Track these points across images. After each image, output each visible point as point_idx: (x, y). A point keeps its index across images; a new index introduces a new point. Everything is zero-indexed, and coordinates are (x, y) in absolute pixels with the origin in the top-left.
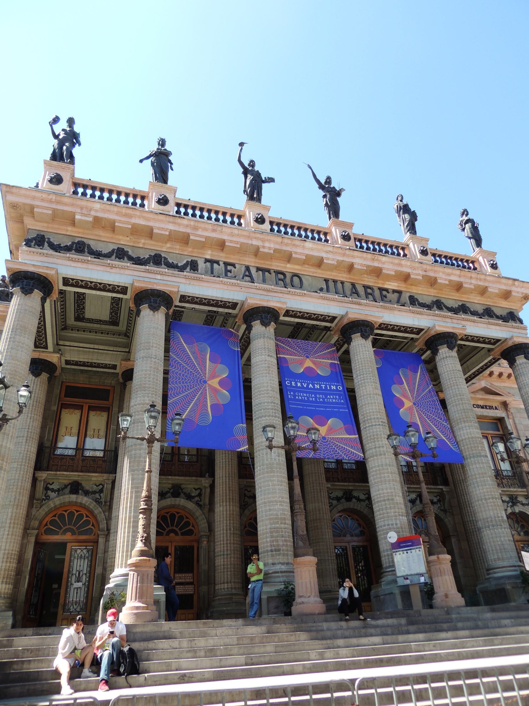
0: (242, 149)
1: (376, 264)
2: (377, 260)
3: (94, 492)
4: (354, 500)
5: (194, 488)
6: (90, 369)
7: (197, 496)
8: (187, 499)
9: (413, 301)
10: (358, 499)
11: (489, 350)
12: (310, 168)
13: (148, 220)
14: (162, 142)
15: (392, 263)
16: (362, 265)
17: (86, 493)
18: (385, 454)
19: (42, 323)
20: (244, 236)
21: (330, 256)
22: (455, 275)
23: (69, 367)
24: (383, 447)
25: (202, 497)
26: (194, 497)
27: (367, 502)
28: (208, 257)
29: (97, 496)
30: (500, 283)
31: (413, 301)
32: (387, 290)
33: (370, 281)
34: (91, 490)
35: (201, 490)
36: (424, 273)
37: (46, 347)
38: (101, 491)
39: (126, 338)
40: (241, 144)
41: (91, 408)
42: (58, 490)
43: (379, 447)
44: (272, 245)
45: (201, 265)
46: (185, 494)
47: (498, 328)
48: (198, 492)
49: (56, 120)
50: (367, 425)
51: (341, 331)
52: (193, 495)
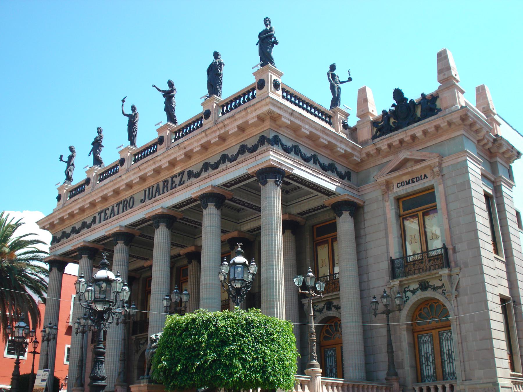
0: (123, 106)
1: (158, 165)
2: (156, 161)
9: (191, 175)
12: (154, 86)
13: (71, 208)
14: (99, 131)
15: (164, 157)
16: (151, 171)
20: (99, 192)
21: (135, 176)
22: (203, 137)
28: (99, 210)
30: (236, 120)
31: (191, 175)
32: (175, 176)
33: (165, 175)
36: (184, 151)
40: (123, 101)
44: (111, 189)
45: (98, 217)
47: (244, 164)
49: (61, 157)
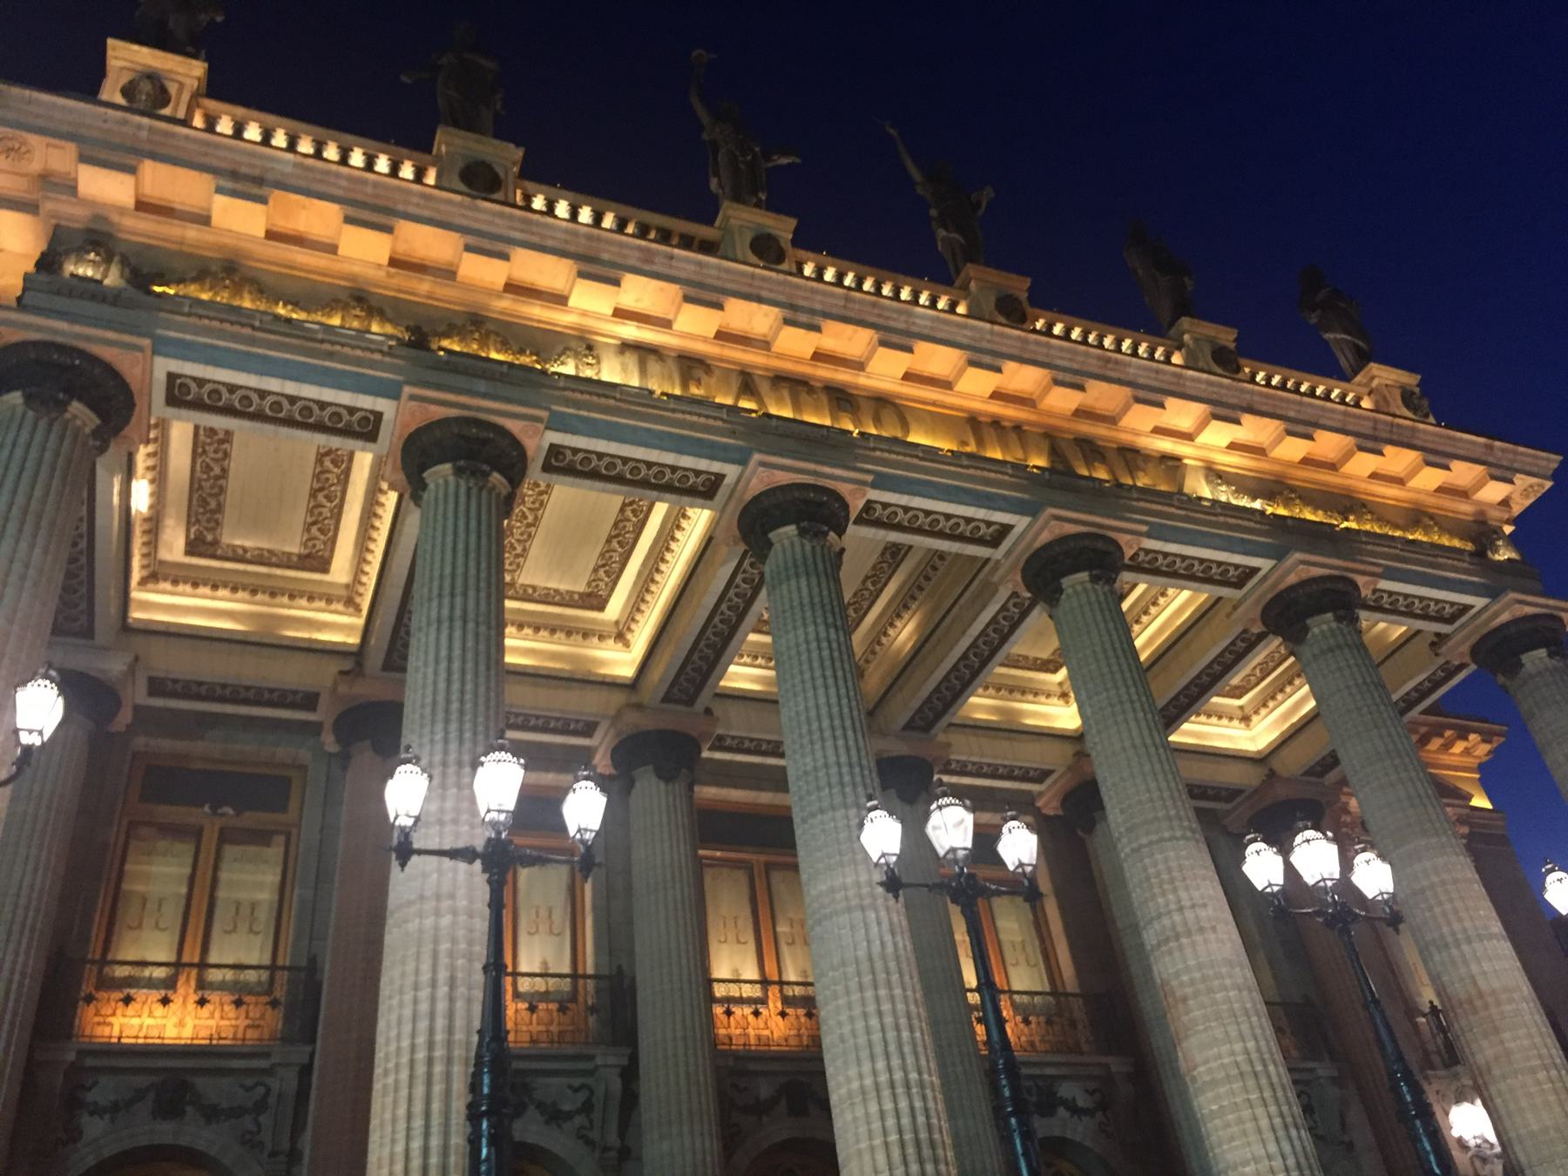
3: (237, 1112)
4: (1062, 1111)
5: (570, 1087)
6: (229, 709)
7: (578, 1112)
8: (547, 1123)
10: (1075, 1110)
11: (1441, 638)
17: (212, 1114)
18: (1214, 929)
19: (83, 560)
23: (159, 702)
24: (1205, 905)
25: (597, 1116)
26: (569, 1116)
27: (1099, 1115)
29: (248, 1122)
34: (225, 1105)
35: (592, 1092)
37: (89, 633)
38: (260, 1107)
39: (351, 610)
41: (227, 837)
42: (115, 1108)
43: (1193, 906)
46: (540, 1106)
48: (581, 1097)
50: (1144, 841)
51: (1024, 571)
52: (566, 1107)
